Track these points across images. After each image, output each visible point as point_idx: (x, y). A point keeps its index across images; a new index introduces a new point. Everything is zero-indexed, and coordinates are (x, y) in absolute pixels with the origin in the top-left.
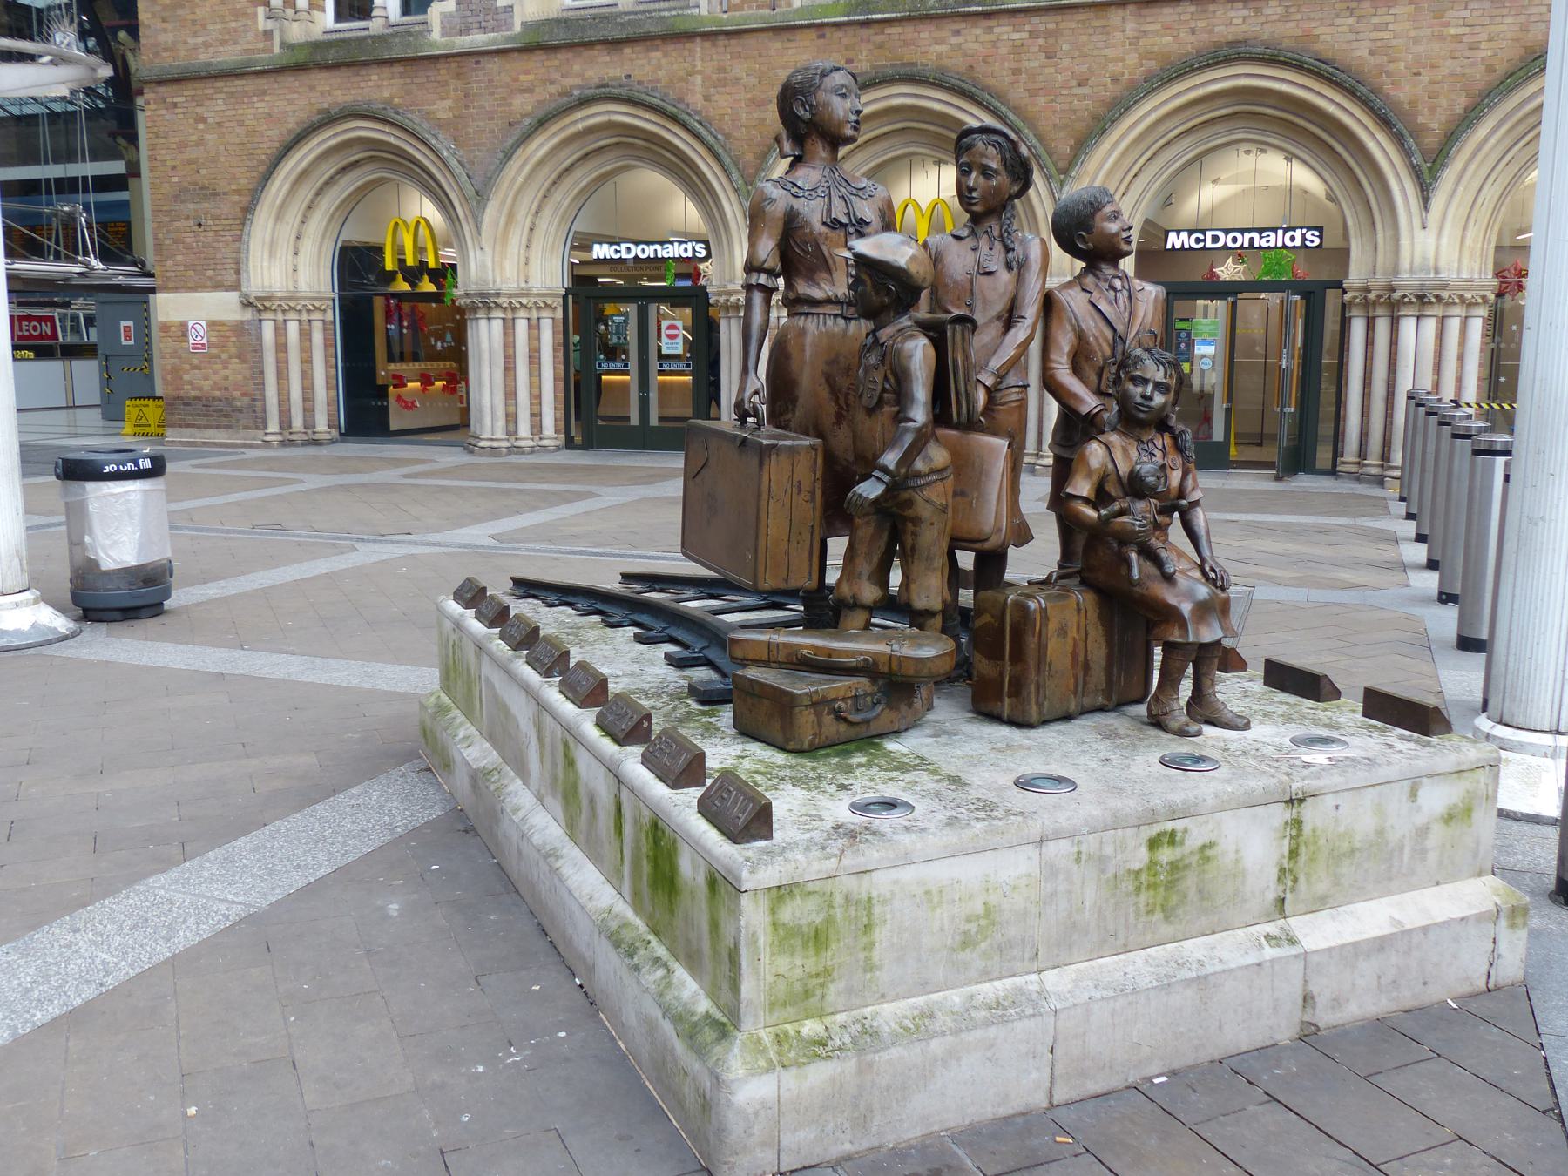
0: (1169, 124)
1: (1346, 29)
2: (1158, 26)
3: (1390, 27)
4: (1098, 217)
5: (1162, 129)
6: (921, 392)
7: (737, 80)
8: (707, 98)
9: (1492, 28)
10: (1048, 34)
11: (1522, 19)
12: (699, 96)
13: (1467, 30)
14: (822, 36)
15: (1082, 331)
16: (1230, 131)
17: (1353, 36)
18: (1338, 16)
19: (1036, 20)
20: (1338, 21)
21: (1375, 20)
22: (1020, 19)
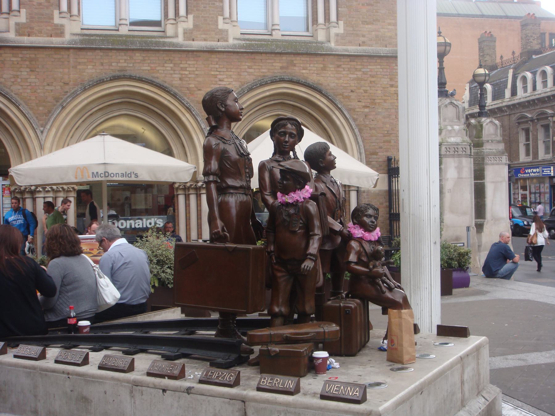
0: (93, 106)
1: (169, 69)
2: (86, 61)
3: (188, 69)
5: (89, 108)
9: (227, 73)
10: (31, 60)
11: (239, 70)
13: (218, 73)
16: (119, 110)
17: (172, 72)
18: (166, 63)
19: (25, 52)
20: (166, 65)
21: (182, 66)
22: (15, 51)
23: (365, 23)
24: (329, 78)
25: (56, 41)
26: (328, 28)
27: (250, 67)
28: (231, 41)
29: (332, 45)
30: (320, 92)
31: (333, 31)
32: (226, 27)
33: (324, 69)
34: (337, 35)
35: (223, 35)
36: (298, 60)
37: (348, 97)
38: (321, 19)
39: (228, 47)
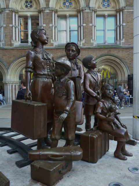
4: (92, 60)
6: (73, 93)
7: (6, 55)
8: (2, 57)
12: (1, 57)
14: (18, 50)
15: (90, 80)
23: (130, 39)
24: (121, 54)
25: (52, 47)
26: (120, 41)
27: (99, 52)
28: (94, 46)
29: (121, 45)
30: (117, 58)
31: (122, 42)
32: (93, 42)
33: (119, 52)
34: (122, 43)
35: (92, 44)
36: (112, 50)
37: (125, 59)
38: (118, 39)
39: (93, 47)
